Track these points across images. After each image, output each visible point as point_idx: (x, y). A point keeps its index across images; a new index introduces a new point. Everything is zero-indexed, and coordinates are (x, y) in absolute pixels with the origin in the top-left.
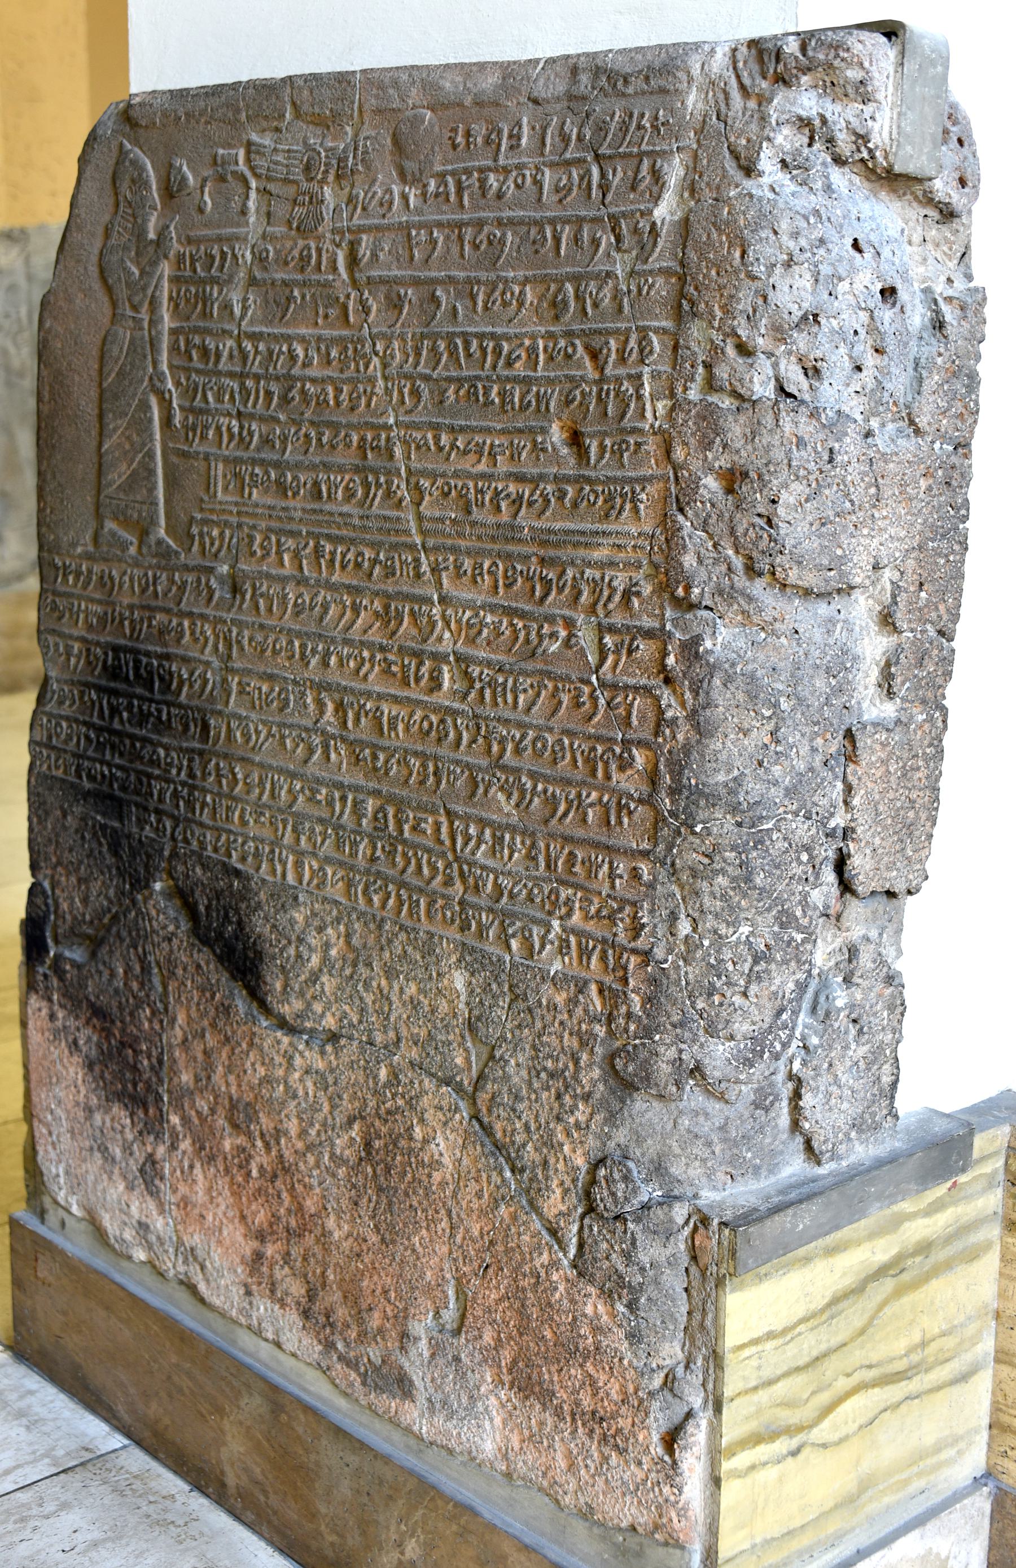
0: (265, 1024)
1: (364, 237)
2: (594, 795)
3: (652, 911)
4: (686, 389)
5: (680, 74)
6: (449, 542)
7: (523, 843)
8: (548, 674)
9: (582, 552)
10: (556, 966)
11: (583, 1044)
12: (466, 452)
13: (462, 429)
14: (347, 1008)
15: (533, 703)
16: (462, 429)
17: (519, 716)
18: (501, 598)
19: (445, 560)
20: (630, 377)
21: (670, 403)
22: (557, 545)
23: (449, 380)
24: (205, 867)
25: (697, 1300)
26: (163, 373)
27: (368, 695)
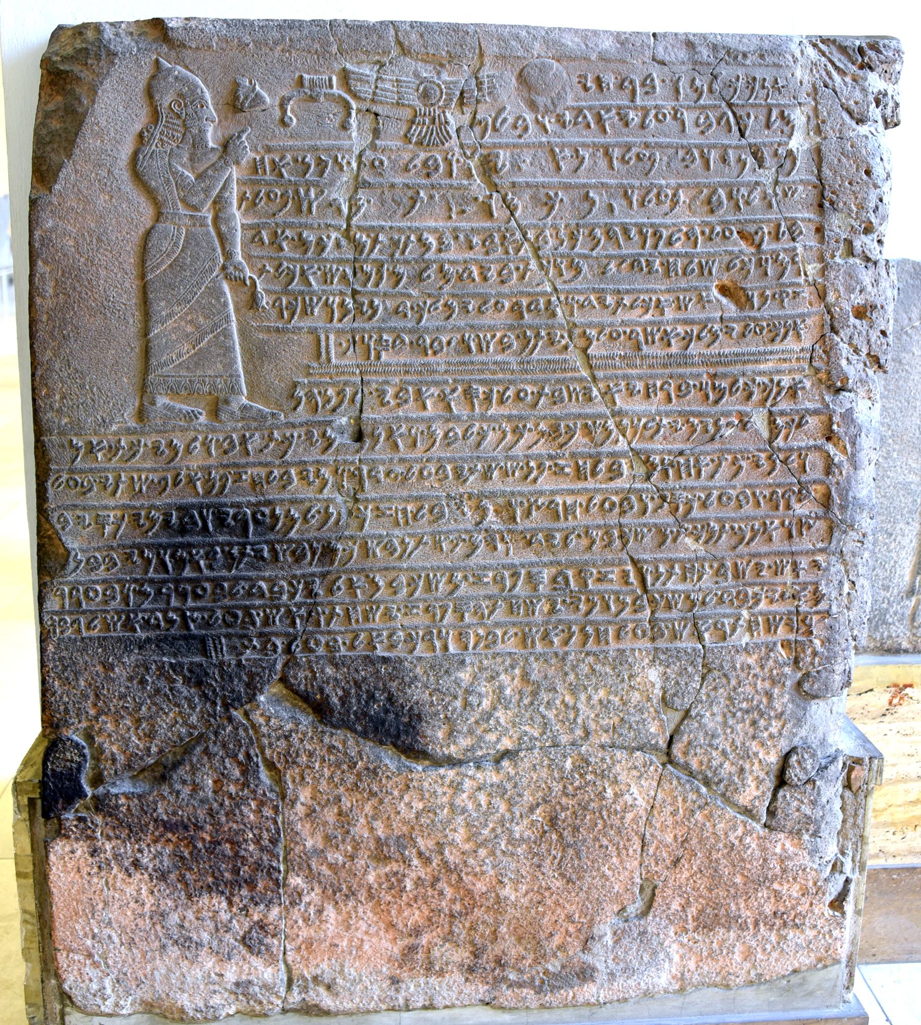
0: (420, 768)
1: (501, 152)
2: (777, 522)
3: (827, 585)
4: (833, 256)
5: (787, 56)
6: (619, 372)
7: (711, 567)
8: (729, 451)
9: (749, 367)
10: (746, 639)
11: (774, 682)
12: (632, 307)
13: (628, 292)
14: (527, 728)
15: (716, 472)
16: (628, 292)
17: (703, 481)
18: (675, 405)
19: (616, 385)
20: (785, 250)
21: (819, 266)
22: (726, 364)
23: (610, 257)
24: (336, 666)
25: (850, 810)
26: (240, 263)
27: (541, 493)
